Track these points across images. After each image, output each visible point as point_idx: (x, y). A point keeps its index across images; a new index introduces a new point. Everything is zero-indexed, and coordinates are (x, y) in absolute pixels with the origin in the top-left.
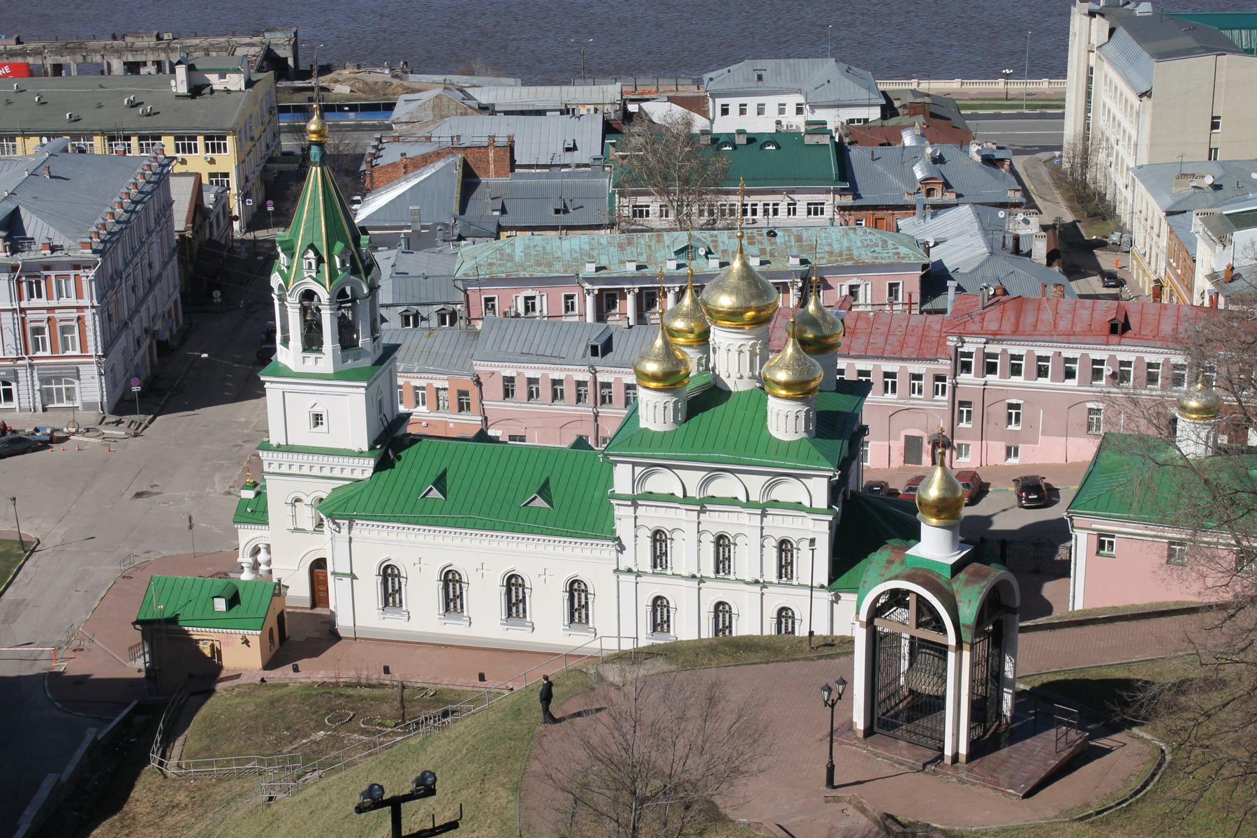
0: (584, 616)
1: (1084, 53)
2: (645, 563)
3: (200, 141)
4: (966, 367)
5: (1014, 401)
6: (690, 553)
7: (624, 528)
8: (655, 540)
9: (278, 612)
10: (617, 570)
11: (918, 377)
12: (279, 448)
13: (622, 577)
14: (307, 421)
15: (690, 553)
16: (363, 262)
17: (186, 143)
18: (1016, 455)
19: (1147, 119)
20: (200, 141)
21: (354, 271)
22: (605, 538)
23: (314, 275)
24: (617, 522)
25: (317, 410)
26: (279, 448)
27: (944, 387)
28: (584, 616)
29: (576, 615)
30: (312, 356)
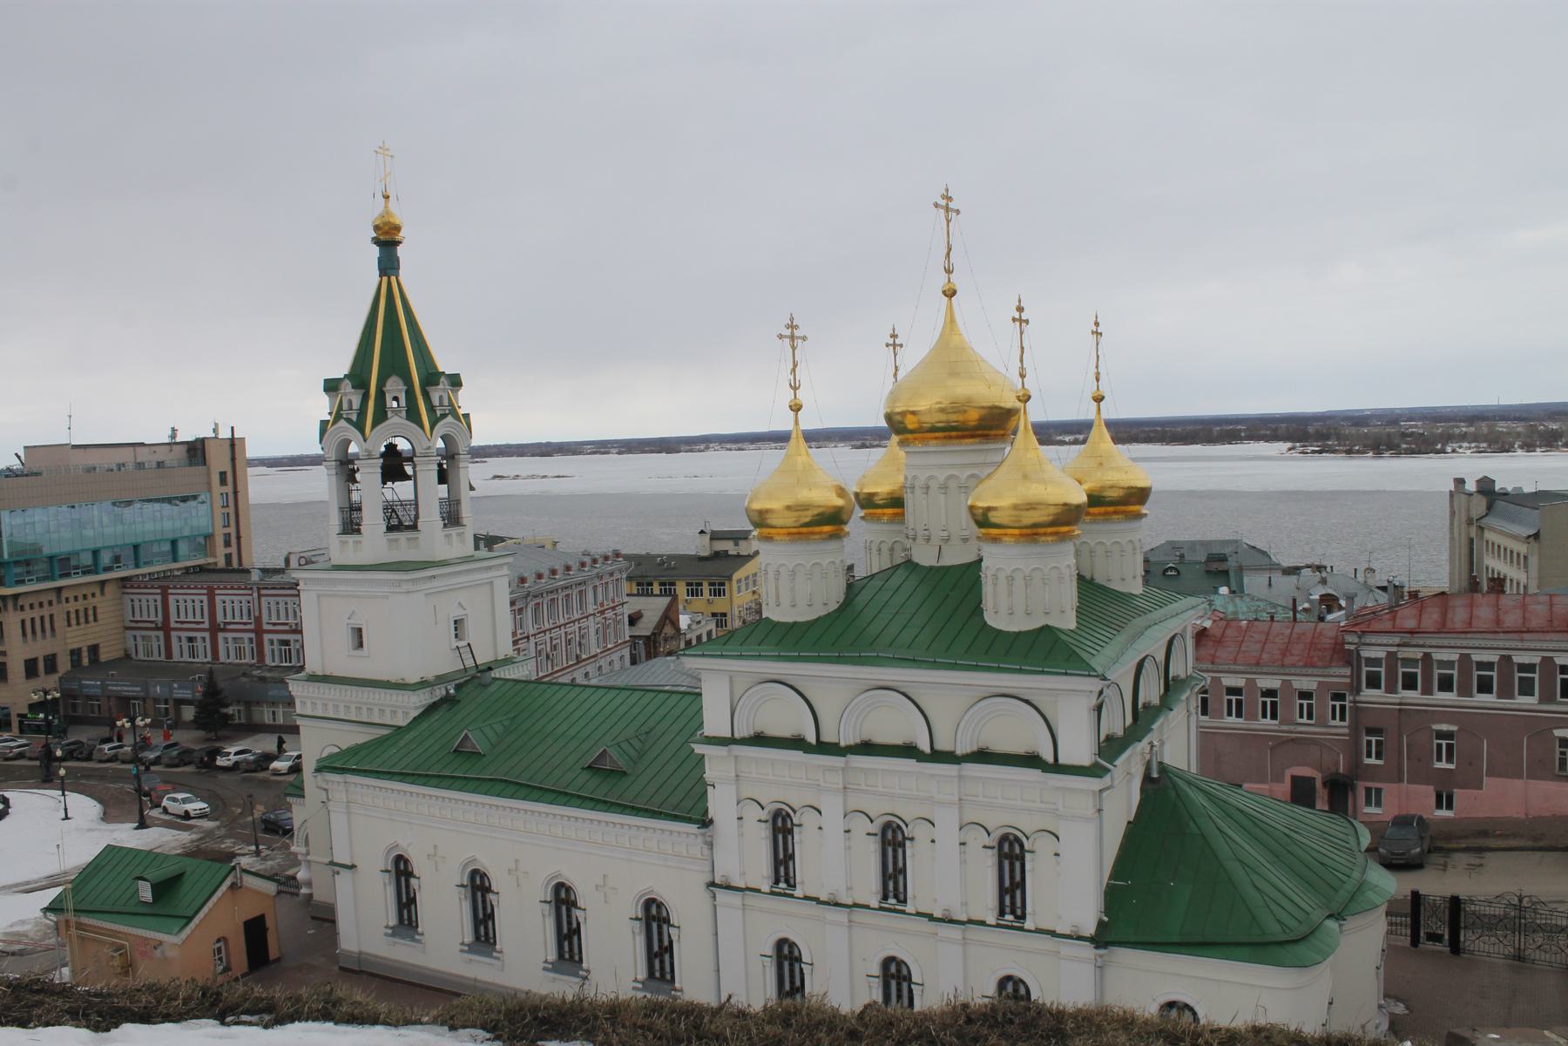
0: (668, 969)
1: (1464, 526)
2: (759, 871)
3: (706, 588)
4: (1374, 682)
5: (1444, 727)
6: (836, 859)
7: (720, 803)
8: (775, 831)
9: (252, 914)
10: (712, 884)
11: (1305, 695)
12: (314, 678)
13: (722, 896)
14: (347, 638)
15: (836, 859)
16: (431, 409)
17: (695, 591)
18: (1450, 806)
19: (1534, 561)
20: (706, 588)
21: (413, 415)
22: (689, 820)
23: (354, 418)
24: (710, 789)
25: (356, 622)
26: (314, 678)
27: (1343, 708)
28: (668, 969)
29: (657, 962)
30: (351, 539)
